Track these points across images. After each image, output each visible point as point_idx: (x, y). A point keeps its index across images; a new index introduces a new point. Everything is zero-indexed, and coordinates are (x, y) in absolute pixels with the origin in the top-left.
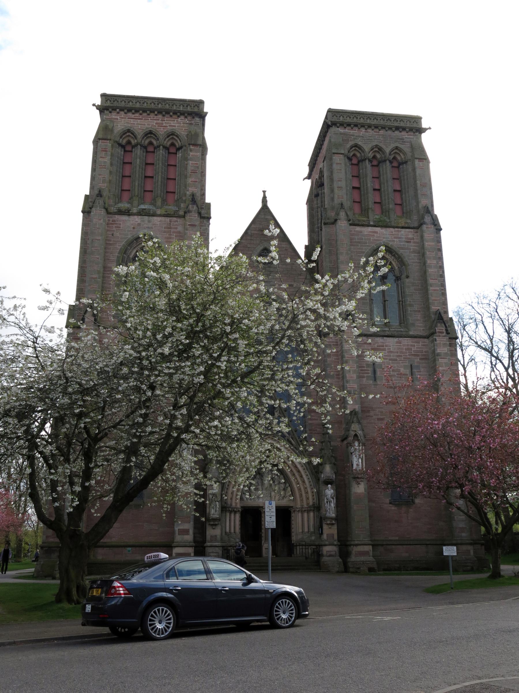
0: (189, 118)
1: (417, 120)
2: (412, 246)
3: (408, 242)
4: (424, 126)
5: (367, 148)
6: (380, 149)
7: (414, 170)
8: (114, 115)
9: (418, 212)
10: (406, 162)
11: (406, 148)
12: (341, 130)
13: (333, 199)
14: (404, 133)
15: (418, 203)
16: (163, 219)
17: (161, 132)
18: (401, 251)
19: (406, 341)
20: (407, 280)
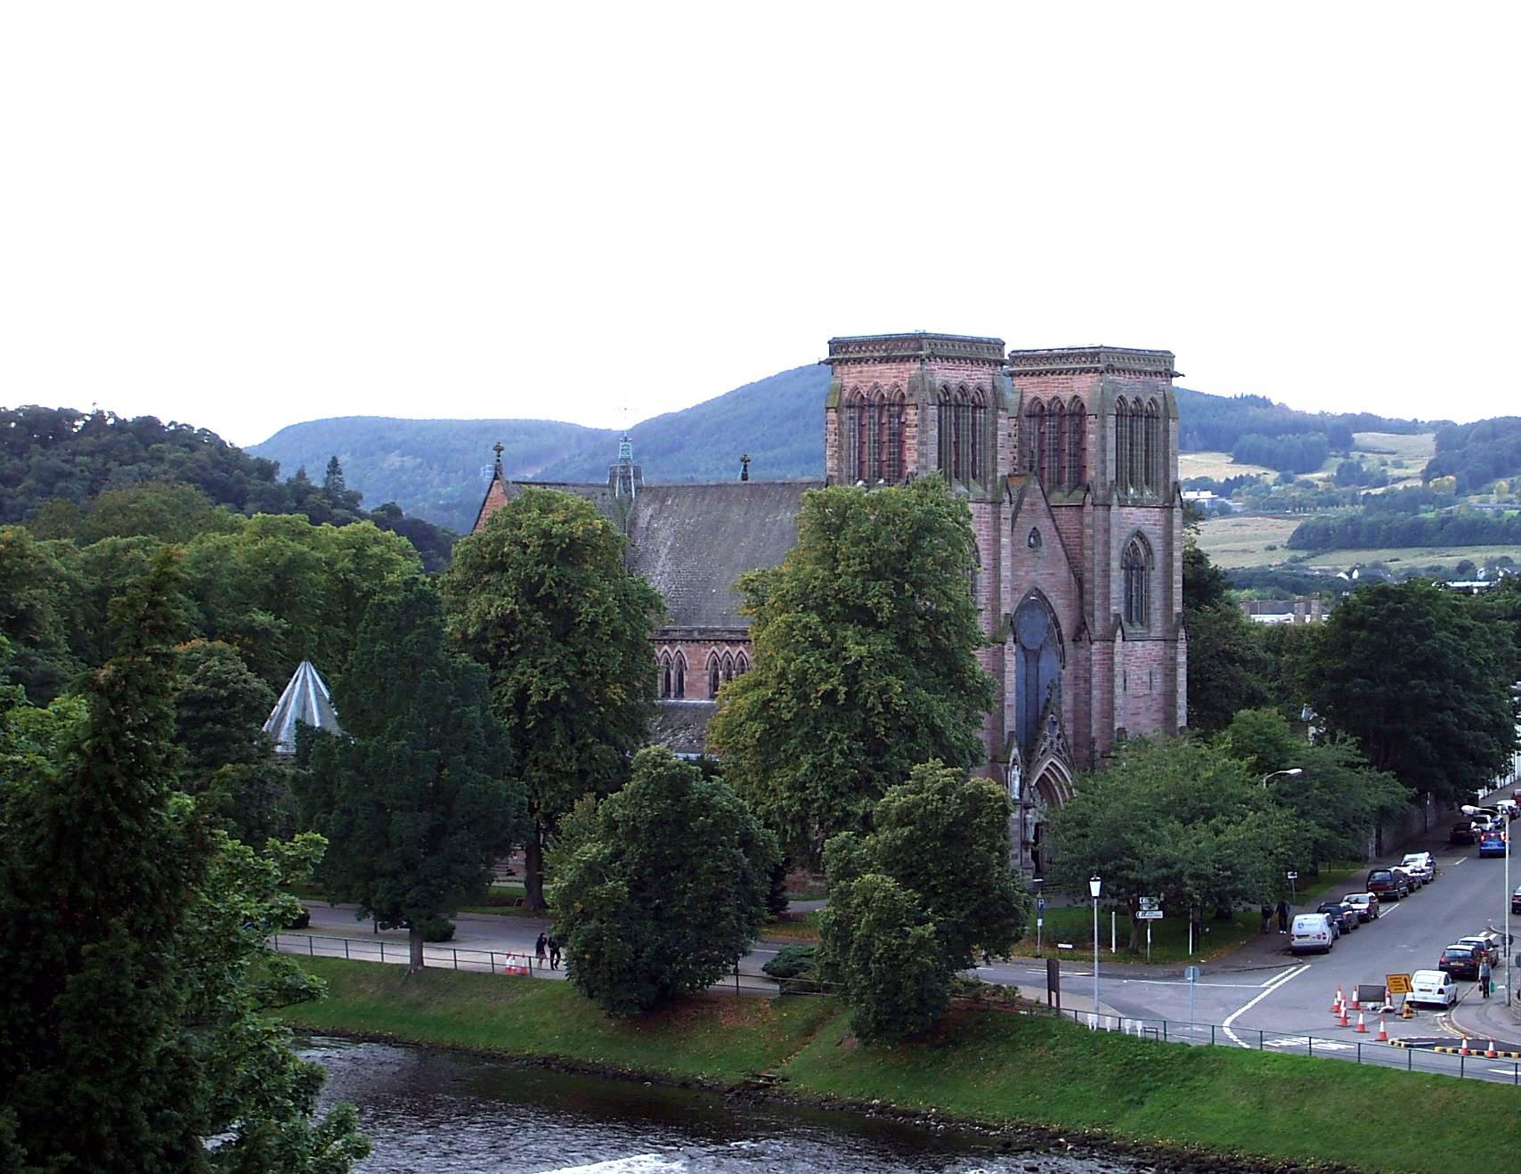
0: (993, 367)
1: (1167, 357)
2: (1159, 530)
3: (1155, 525)
4: (1175, 370)
5: (1130, 400)
6: (1138, 400)
7: (1166, 430)
8: (933, 366)
9: (1166, 487)
10: (1157, 418)
11: (1159, 398)
12: (1110, 377)
13: (1104, 473)
14: (1159, 378)
15: (1167, 475)
16: (975, 505)
17: (972, 385)
18: (1150, 537)
19: (1149, 645)
20: (1152, 573)
